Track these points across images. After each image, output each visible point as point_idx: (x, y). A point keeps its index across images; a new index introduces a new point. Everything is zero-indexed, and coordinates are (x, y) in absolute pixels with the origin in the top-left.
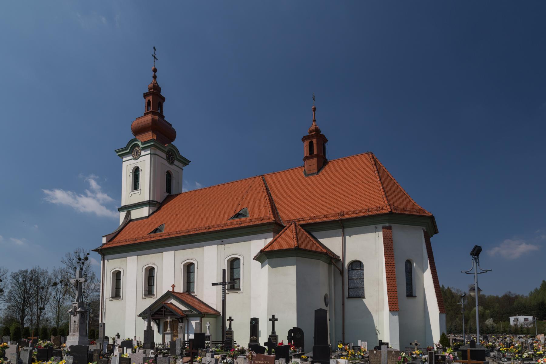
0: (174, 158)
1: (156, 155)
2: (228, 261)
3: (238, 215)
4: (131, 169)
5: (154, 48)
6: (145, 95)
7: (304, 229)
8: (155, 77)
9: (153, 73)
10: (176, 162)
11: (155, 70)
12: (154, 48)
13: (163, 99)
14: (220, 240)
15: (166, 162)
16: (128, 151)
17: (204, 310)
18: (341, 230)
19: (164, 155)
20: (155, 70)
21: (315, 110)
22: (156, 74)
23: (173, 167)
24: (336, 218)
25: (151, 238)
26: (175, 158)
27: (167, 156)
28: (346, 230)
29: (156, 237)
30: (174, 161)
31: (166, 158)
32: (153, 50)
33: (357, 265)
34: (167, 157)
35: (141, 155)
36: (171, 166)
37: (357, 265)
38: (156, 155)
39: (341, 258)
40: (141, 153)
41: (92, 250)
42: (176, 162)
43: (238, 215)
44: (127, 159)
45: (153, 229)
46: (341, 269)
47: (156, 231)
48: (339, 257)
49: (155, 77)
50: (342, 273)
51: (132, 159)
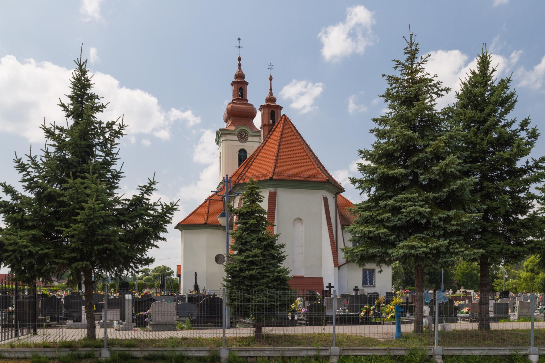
0: (247, 135)
5: (239, 39)
8: (240, 65)
9: (238, 62)
10: (250, 139)
11: (239, 59)
12: (239, 39)
15: (238, 143)
19: (236, 138)
20: (239, 59)
22: (241, 62)
23: (247, 144)
26: (249, 135)
27: (239, 136)
30: (248, 138)
31: (237, 139)
32: (238, 41)
34: (238, 138)
36: (244, 144)
42: (250, 139)
49: (240, 65)
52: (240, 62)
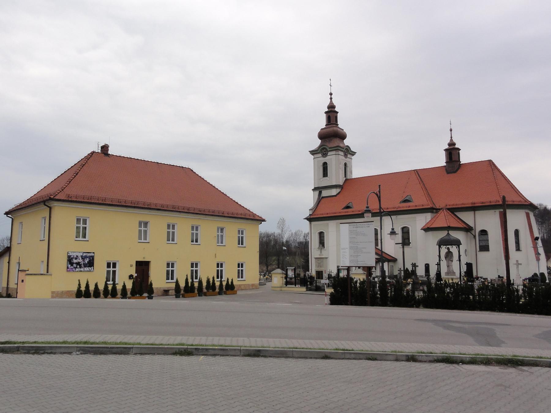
1: (339, 155)
2: (401, 228)
3: (406, 201)
4: (321, 164)
6: (326, 113)
7: (450, 211)
8: (331, 99)
11: (331, 94)
13: (337, 113)
14: (395, 216)
16: (319, 152)
17: (390, 258)
18: (473, 212)
20: (331, 94)
21: (451, 130)
24: (470, 205)
25: (346, 212)
28: (477, 212)
29: (350, 212)
33: (484, 233)
35: (328, 155)
37: (484, 233)
38: (339, 155)
39: (474, 228)
40: (328, 153)
41: (304, 219)
43: (406, 201)
44: (318, 157)
45: (344, 206)
46: (474, 234)
47: (348, 207)
48: (472, 227)
49: (331, 99)
50: (475, 237)
51: (321, 157)
52: (331, 96)
